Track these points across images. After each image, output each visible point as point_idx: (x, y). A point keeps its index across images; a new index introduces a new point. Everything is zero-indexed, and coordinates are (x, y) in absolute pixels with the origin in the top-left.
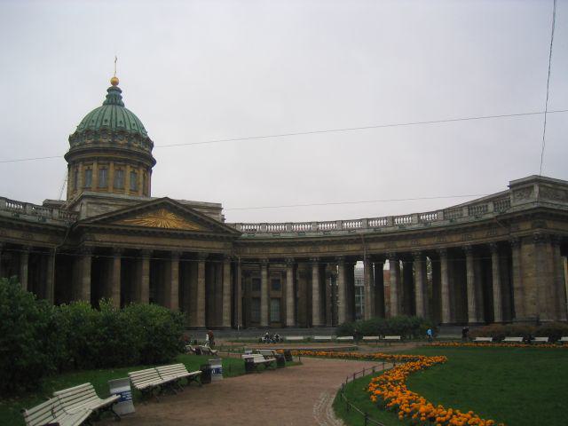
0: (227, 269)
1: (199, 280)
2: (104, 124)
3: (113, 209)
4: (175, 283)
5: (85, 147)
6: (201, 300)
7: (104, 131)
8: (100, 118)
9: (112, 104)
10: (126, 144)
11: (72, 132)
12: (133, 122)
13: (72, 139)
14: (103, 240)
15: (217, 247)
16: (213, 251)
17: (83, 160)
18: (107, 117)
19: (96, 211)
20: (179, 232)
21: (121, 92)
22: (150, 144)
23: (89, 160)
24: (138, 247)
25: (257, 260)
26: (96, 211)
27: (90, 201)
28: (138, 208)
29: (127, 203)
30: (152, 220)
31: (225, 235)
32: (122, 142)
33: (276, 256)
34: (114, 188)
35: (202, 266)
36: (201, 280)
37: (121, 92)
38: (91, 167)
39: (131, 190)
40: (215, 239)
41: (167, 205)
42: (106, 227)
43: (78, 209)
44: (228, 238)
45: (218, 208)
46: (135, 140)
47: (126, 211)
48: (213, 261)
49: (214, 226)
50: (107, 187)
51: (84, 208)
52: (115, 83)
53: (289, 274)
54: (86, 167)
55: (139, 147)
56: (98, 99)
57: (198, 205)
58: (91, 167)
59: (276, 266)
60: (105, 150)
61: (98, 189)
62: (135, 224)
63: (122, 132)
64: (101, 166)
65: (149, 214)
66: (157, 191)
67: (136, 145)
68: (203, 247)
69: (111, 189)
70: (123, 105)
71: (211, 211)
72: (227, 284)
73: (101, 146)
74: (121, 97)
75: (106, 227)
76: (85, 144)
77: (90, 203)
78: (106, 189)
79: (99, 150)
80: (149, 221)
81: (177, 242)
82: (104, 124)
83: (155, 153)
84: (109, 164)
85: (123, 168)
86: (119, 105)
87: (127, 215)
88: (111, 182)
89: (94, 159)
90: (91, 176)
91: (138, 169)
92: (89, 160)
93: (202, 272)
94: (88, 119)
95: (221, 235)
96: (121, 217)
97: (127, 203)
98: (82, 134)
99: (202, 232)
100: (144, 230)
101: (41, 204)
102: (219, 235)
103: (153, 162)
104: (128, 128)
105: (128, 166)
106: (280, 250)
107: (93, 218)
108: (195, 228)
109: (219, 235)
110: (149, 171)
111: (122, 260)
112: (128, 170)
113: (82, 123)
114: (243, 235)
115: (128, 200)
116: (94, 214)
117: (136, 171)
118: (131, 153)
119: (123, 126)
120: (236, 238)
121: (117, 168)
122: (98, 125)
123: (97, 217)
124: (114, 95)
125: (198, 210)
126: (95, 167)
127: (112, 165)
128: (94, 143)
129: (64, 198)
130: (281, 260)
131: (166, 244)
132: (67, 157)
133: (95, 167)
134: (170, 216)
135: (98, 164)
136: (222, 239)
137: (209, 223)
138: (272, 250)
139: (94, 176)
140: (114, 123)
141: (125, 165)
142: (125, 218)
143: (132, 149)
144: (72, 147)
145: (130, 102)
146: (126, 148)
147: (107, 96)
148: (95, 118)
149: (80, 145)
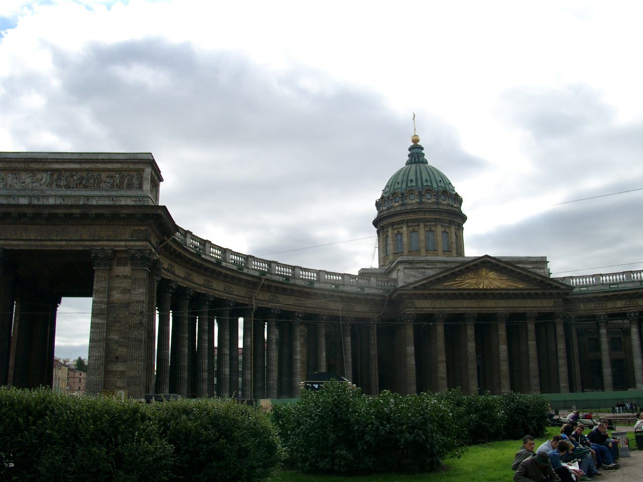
0: (560, 330)
1: (530, 343)
2: (409, 185)
3: (430, 272)
4: (503, 348)
5: (393, 210)
6: (533, 365)
7: (411, 191)
8: (405, 178)
9: (415, 163)
10: (433, 203)
11: (379, 197)
12: (439, 179)
13: (378, 205)
14: (425, 305)
15: (546, 305)
16: (543, 310)
17: (392, 224)
18: (412, 177)
19: (415, 276)
20: (503, 292)
21: (423, 149)
22: (458, 200)
23: (398, 223)
24: (461, 311)
25: (594, 316)
26: (415, 276)
27: (407, 266)
28: (457, 270)
29: (444, 265)
30: (474, 281)
32: (429, 200)
33: (616, 311)
34: (426, 251)
35: (531, 327)
36: (532, 344)
37: (423, 149)
38: (400, 230)
39: (444, 251)
40: (544, 296)
41: (486, 263)
42: (426, 292)
43: (394, 275)
44: (558, 294)
45: (543, 262)
46: (442, 197)
47: (446, 274)
48: (544, 321)
49: (542, 282)
50: (420, 251)
51: (401, 274)
52: (416, 141)
53: (634, 330)
54: (396, 231)
55: (448, 205)
56: (401, 160)
57: (521, 261)
58: (400, 230)
59: (615, 321)
60: (414, 212)
61: (410, 252)
62: (454, 287)
63: (429, 190)
64: (411, 229)
65: (471, 275)
66: (471, 251)
67: (445, 202)
69: (423, 251)
70: (426, 162)
71: (535, 266)
72: (561, 346)
73: (409, 207)
74: (423, 155)
75: (426, 292)
76: (392, 207)
77: (405, 268)
78: (418, 251)
79: (407, 213)
80: (469, 282)
81: (503, 303)
82: (409, 185)
83: (464, 209)
84: (419, 225)
85: (433, 228)
86: (419, 162)
87: (446, 279)
88: (423, 245)
89: (402, 222)
90: (401, 240)
91: (449, 227)
92: (398, 223)
93: (532, 335)
95: (551, 291)
96: (439, 281)
97: (444, 265)
98: (388, 198)
99: (535, 289)
100: (466, 292)
101: (357, 274)
102: (547, 292)
103: (464, 218)
104: (435, 186)
105: (439, 226)
106: (620, 304)
107: (411, 284)
108: (521, 286)
109: (547, 292)
110: (460, 228)
111: (446, 327)
112: (439, 229)
113: (387, 186)
114: (575, 290)
115: (446, 262)
116: (412, 280)
118: (440, 212)
119: (430, 184)
120: (567, 294)
122: (404, 186)
123: (416, 282)
124: (416, 154)
125: (520, 266)
126: (405, 229)
127: (422, 226)
128: (402, 205)
129: (376, 265)
130: (623, 315)
131: (490, 305)
132: (375, 223)
133: (405, 229)
134: (492, 275)
135: (408, 227)
136: (551, 296)
137: (535, 279)
138: (610, 305)
139: (405, 239)
140: (419, 182)
141: (436, 226)
142: (445, 281)
143: (441, 207)
144: (379, 213)
145: (432, 159)
146: (435, 207)
147: (409, 156)
148: (399, 180)
149: (387, 210)
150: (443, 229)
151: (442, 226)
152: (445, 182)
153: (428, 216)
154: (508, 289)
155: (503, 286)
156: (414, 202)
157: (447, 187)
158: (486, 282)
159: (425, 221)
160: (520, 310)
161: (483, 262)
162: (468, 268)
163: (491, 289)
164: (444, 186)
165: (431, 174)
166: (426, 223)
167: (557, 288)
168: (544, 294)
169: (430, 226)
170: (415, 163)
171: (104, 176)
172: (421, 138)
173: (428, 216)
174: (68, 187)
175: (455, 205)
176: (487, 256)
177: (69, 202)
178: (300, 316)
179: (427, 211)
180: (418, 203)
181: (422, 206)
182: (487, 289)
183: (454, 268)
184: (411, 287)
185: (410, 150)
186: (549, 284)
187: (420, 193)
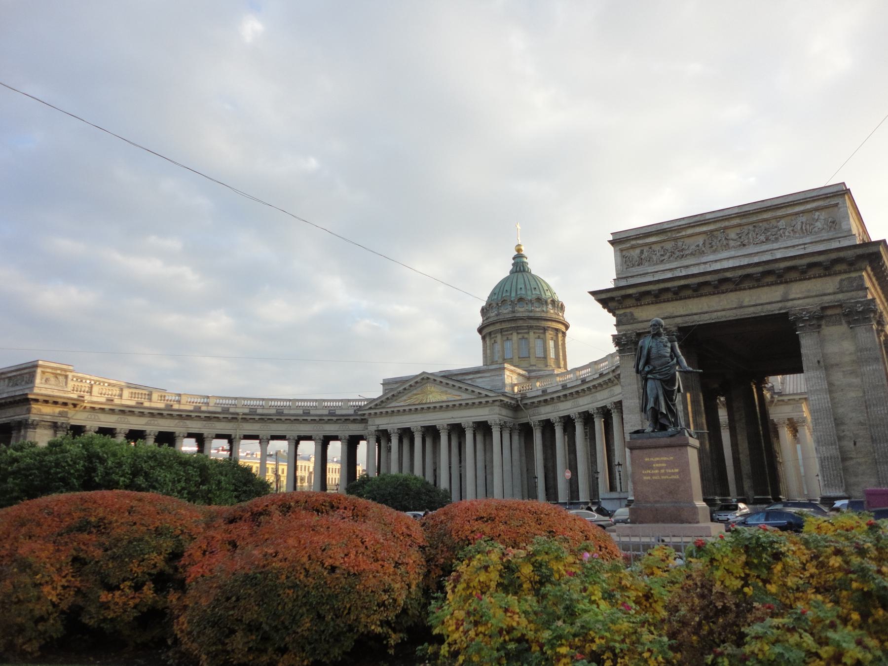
9: (520, 271)
10: (508, 313)
14: (383, 423)
18: (497, 291)
31: (483, 400)
32: (506, 311)
42: (378, 411)
44: (487, 402)
52: (519, 250)
60: (493, 324)
65: (419, 390)
67: (520, 310)
68: (467, 417)
75: (378, 411)
84: (496, 337)
85: (510, 337)
94: (493, 293)
102: (477, 401)
104: (513, 294)
105: (515, 334)
112: (515, 337)
117: (526, 336)
121: (505, 338)
135: (491, 339)
140: (500, 293)
143: (518, 315)
145: (535, 265)
146: (510, 316)
150: (520, 336)
151: (518, 333)
152: (528, 287)
153: (504, 326)
154: (448, 401)
155: (444, 398)
156: (494, 314)
157: (529, 293)
158: (431, 396)
159: (501, 331)
160: (457, 421)
161: (423, 379)
162: (411, 386)
163: (433, 403)
164: (523, 292)
165: (514, 284)
166: (504, 333)
167: (487, 396)
168: (480, 403)
169: (507, 335)
170: (516, 272)
171: (25, 376)
172: (523, 248)
173: (504, 326)
174: (12, 386)
175: (537, 309)
176: (424, 373)
177: (13, 394)
178: (291, 438)
179: (504, 321)
180: (497, 315)
181: (500, 317)
182: (430, 403)
183: (398, 387)
184: (367, 407)
185: (514, 259)
186: (480, 393)
187: (497, 304)
